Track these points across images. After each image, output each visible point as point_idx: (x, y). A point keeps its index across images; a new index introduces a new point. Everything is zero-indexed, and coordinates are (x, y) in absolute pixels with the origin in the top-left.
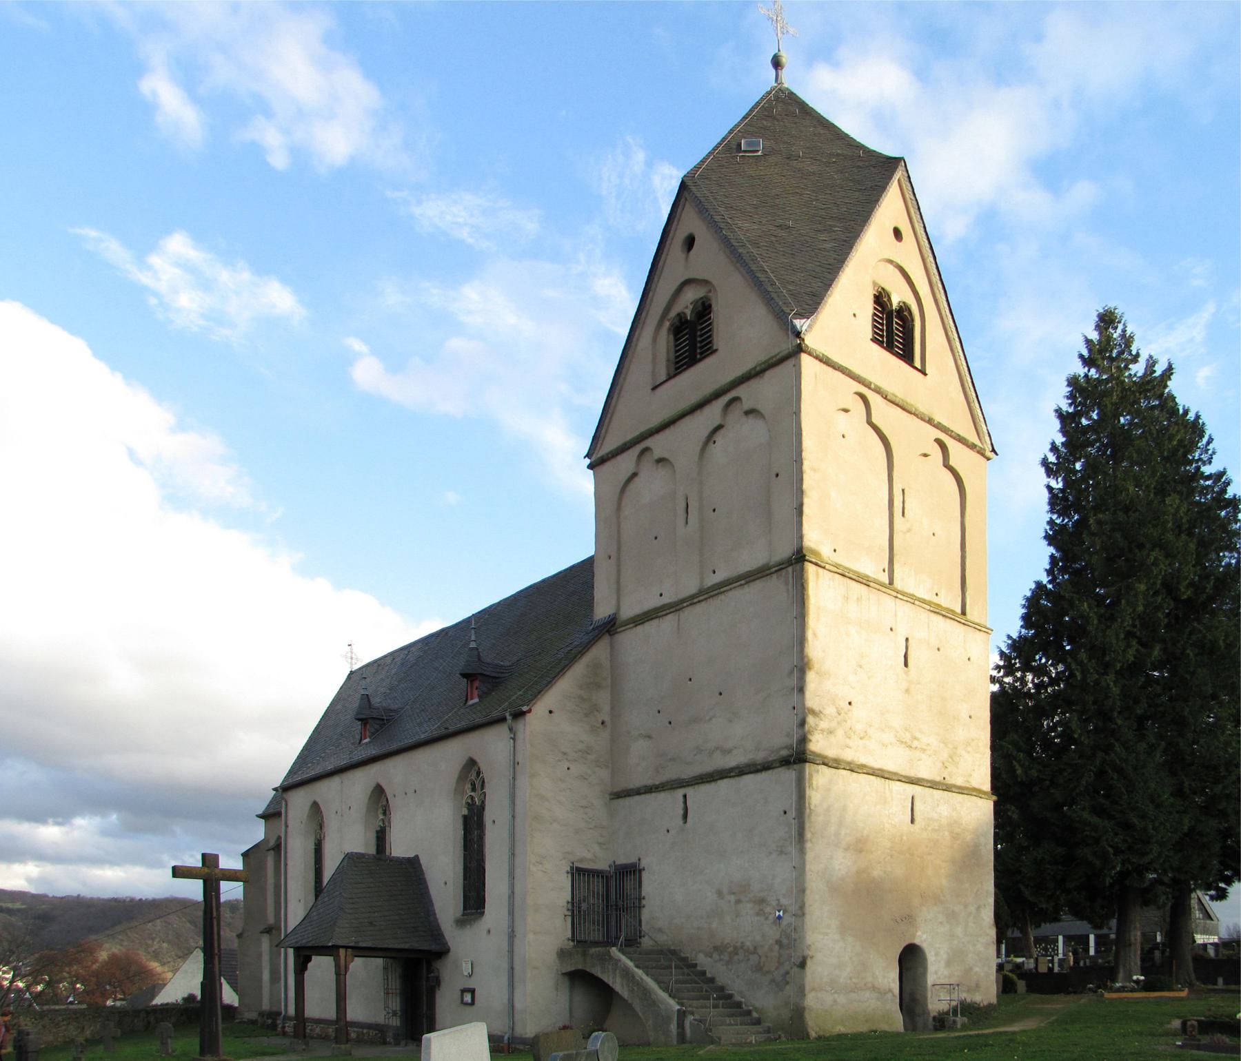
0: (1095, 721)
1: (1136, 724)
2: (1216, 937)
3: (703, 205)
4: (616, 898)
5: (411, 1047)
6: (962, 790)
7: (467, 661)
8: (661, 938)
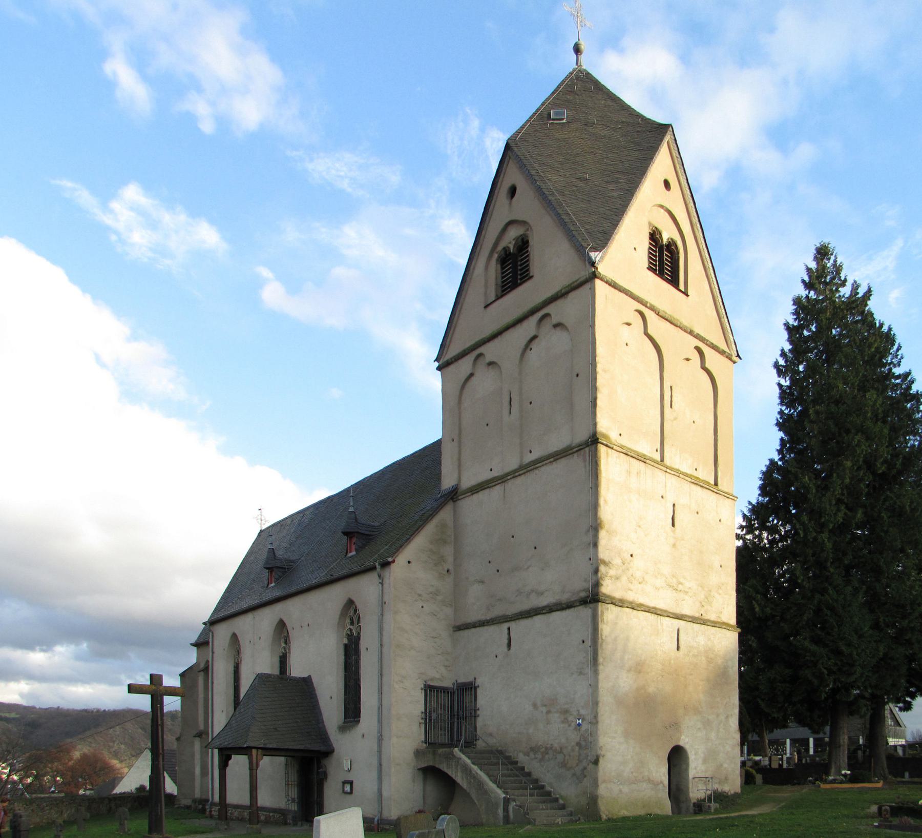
0: (814, 570)
1: (844, 572)
2: (904, 740)
3: (522, 162)
4: (458, 710)
5: (306, 827)
6: (715, 624)
7: (347, 522)
8: (492, 741)
